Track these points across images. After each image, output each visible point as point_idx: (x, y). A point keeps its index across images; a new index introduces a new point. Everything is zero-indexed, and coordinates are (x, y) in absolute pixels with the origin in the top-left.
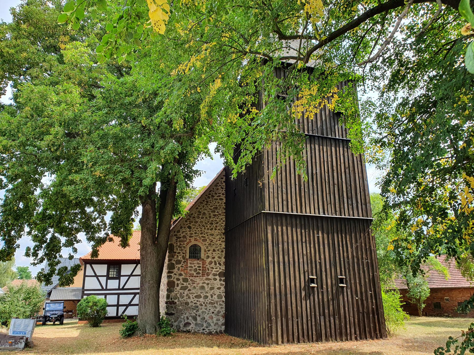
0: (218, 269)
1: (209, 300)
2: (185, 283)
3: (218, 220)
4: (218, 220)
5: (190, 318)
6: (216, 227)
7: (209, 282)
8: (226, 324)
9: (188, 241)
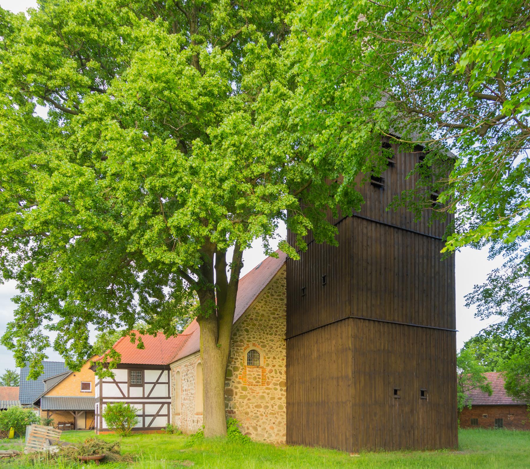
0: (279, 378)
1: (269, 410)
2: (244, 392)
3: (278, 324)
4: (278, 324)
5: (251, 428)
6: (276, 331)
7: (269, 391)
8: (289, 434)
9: (245, 346)
